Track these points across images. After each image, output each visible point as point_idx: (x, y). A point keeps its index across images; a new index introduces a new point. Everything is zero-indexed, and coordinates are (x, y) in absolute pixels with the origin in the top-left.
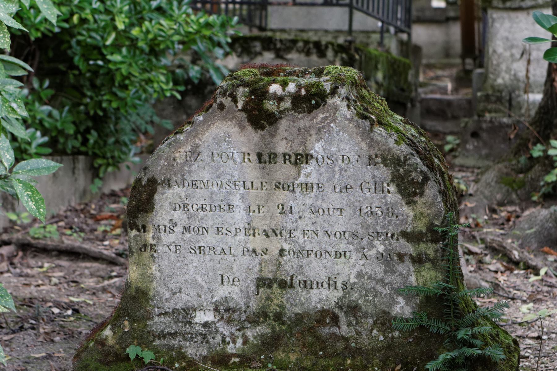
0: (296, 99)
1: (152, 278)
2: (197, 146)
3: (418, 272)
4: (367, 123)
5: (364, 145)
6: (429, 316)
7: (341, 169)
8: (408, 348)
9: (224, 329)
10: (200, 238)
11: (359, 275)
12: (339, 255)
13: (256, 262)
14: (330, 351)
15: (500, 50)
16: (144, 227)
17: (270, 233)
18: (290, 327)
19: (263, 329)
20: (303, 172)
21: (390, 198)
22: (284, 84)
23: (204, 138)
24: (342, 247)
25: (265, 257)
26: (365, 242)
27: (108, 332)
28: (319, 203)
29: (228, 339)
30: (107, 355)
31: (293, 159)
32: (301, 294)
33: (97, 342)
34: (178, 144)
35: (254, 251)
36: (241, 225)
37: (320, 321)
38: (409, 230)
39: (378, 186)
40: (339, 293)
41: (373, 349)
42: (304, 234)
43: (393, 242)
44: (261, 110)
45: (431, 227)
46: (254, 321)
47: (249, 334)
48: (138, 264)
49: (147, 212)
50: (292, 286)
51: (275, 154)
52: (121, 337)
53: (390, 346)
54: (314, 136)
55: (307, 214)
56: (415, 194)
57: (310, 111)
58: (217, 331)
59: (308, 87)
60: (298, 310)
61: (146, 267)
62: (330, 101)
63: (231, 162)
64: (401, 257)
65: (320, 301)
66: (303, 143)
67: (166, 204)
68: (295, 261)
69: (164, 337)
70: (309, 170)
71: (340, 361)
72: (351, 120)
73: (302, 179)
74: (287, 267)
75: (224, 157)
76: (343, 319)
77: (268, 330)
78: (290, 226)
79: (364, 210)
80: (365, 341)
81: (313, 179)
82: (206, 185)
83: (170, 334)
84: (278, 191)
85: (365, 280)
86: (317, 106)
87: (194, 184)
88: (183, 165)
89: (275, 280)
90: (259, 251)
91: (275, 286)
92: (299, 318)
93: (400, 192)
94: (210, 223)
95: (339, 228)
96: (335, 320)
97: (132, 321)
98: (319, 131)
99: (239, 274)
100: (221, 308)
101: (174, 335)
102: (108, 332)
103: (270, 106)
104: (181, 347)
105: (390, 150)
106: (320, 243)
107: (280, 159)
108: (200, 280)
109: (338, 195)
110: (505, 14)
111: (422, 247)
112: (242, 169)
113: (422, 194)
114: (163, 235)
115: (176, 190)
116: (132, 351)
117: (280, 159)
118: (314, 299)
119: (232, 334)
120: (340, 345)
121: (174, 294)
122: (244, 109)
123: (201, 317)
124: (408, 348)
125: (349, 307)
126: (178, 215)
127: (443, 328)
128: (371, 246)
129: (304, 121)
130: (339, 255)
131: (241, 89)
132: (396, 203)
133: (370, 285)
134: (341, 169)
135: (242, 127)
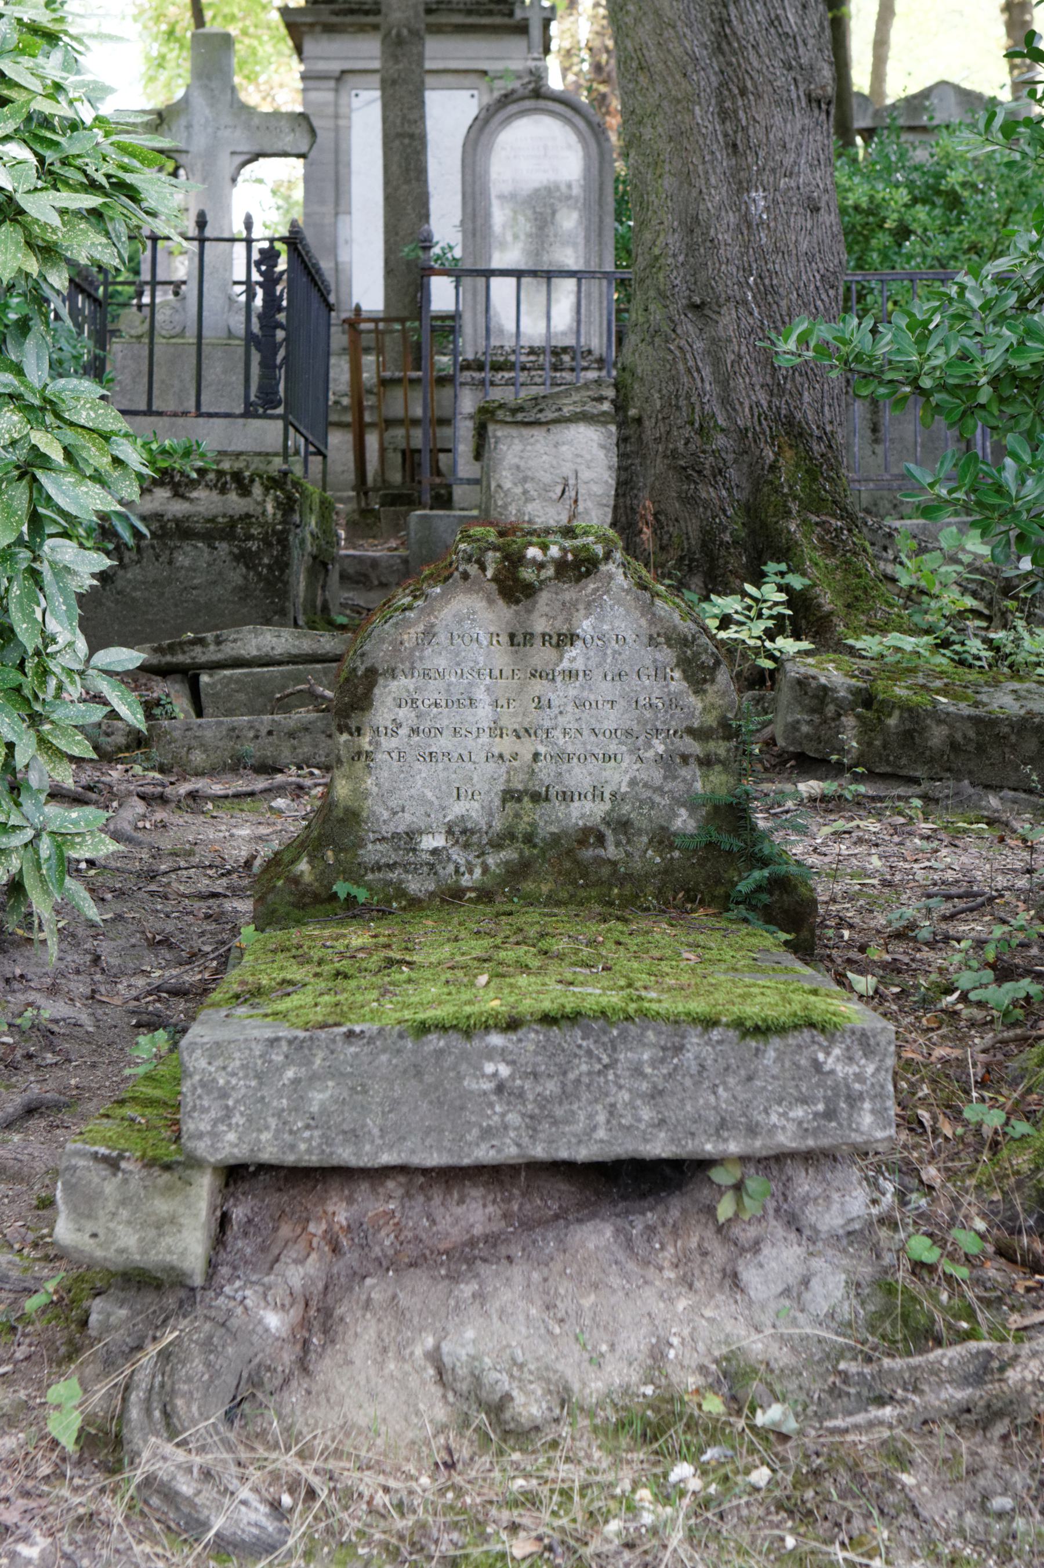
0: (562, 567)
1: (366, 795)
2: (433, 626)
3: (705, 777)
4: (648, 595)
5: (643, 622)
6: (719, 829)
7: (615, 652)
8: (690, 871)
9: (458, 856)
10: (431, 741)
11: (633, 782)
12: (608, 758)
13: (504, 769)
14: (593, 878)
15: (507, 485)
16: (359, 730)
17: (522, 733)
18: (543, 851)
19: (509, 854)
20: (567, 656)
21: (674, 686)
22: (544, 548)
23: (442, 615)
24: (613, 748)
25: (515, 763)
26: (640, 741)
27: (303, 866)
28: (585, 694)
29: (462, 869)
30: (303, 895)
31: (554, 641)
32: (559, 809)
33: (287, 879)
34: (408, 624)
35: (501, 756)
36: (485, 725)
37: (582, 842)
38: (696, 725)
39: (659, 673)
40: (607, 806)
41: (646, 875)
42: (565, 733)
43: (676, 740)
44: (516, 580)
45: (724, 723)
46: (497, 845)
47: (490, 861)
48: (348, 777)
49: (363, 709)
50: (547, 799)
51: (532, 635)
52: (322, 873)
53: (667, 871)
54: (582, 612)
55: (570, 708)
56: (705, 681)
57: (578, 580)
58: (449, 859)
59: (576, 551)
60: (554, 829)
61: (359, 780)
62: (603, 568)
63: (475, 646)
64: (685, 759)
65: (583, 816)
66: (568, 620)
67: (389, 701)
68: (553, 767)
69: (379, 869)
70: (574, 653)
71: (605, 890)
72: (628, 591)
73: (565, 664)
74: (542, 775)
75: (467, 639)
76: (610, 838)
77: (516, 856)
78: (547, 724)
79: (642, 702)
80: (637, 865)
81: (579, 665)
82: (441, 675)
83: (388, 866)
84: (533, 681)
85: (639, 788)
86: (588, 573)
87: (426, 674)
88: (412, 650)
89: (526, 792)
90: (507, 756)
91: (526, 799)
92: (556, 839)
93: (686, 678)
94: (446, 722)
95: (609, 725)
96: (601, 839)
97: (339, 850)
98: (588, 605)
99: (481, 786)
100: (457, 829)
101: (391, 867)
102: (303, 866)
103: (527, 574)
104: (401, 882)
105: (675, 627)
106: (584, 743)
107: (538, 641)
108: (429, 795)
109: (609, 684)
110: (514, 431)
111: (712, 745)
112: (488, 655)
113: (713, 681)
114: (383, 739)
115: (403, 681)
116: (341, 888)
117: (538, 641)
118: (575, 814)
119: (468, 862)
120: (605, 871)
121: (395, 813)
122: (495, 579)
123: (428, 843)
124: (690, 871)
125: (619, 822)
126: (404, 713)
127: (737, 844)
128: (649, 745)
129: (569, 593)
130: (608, 758)
131: (490, 554)
132: (681, 692)
133: (646, 794)
134: (615, 652)
135: (491, 602)
